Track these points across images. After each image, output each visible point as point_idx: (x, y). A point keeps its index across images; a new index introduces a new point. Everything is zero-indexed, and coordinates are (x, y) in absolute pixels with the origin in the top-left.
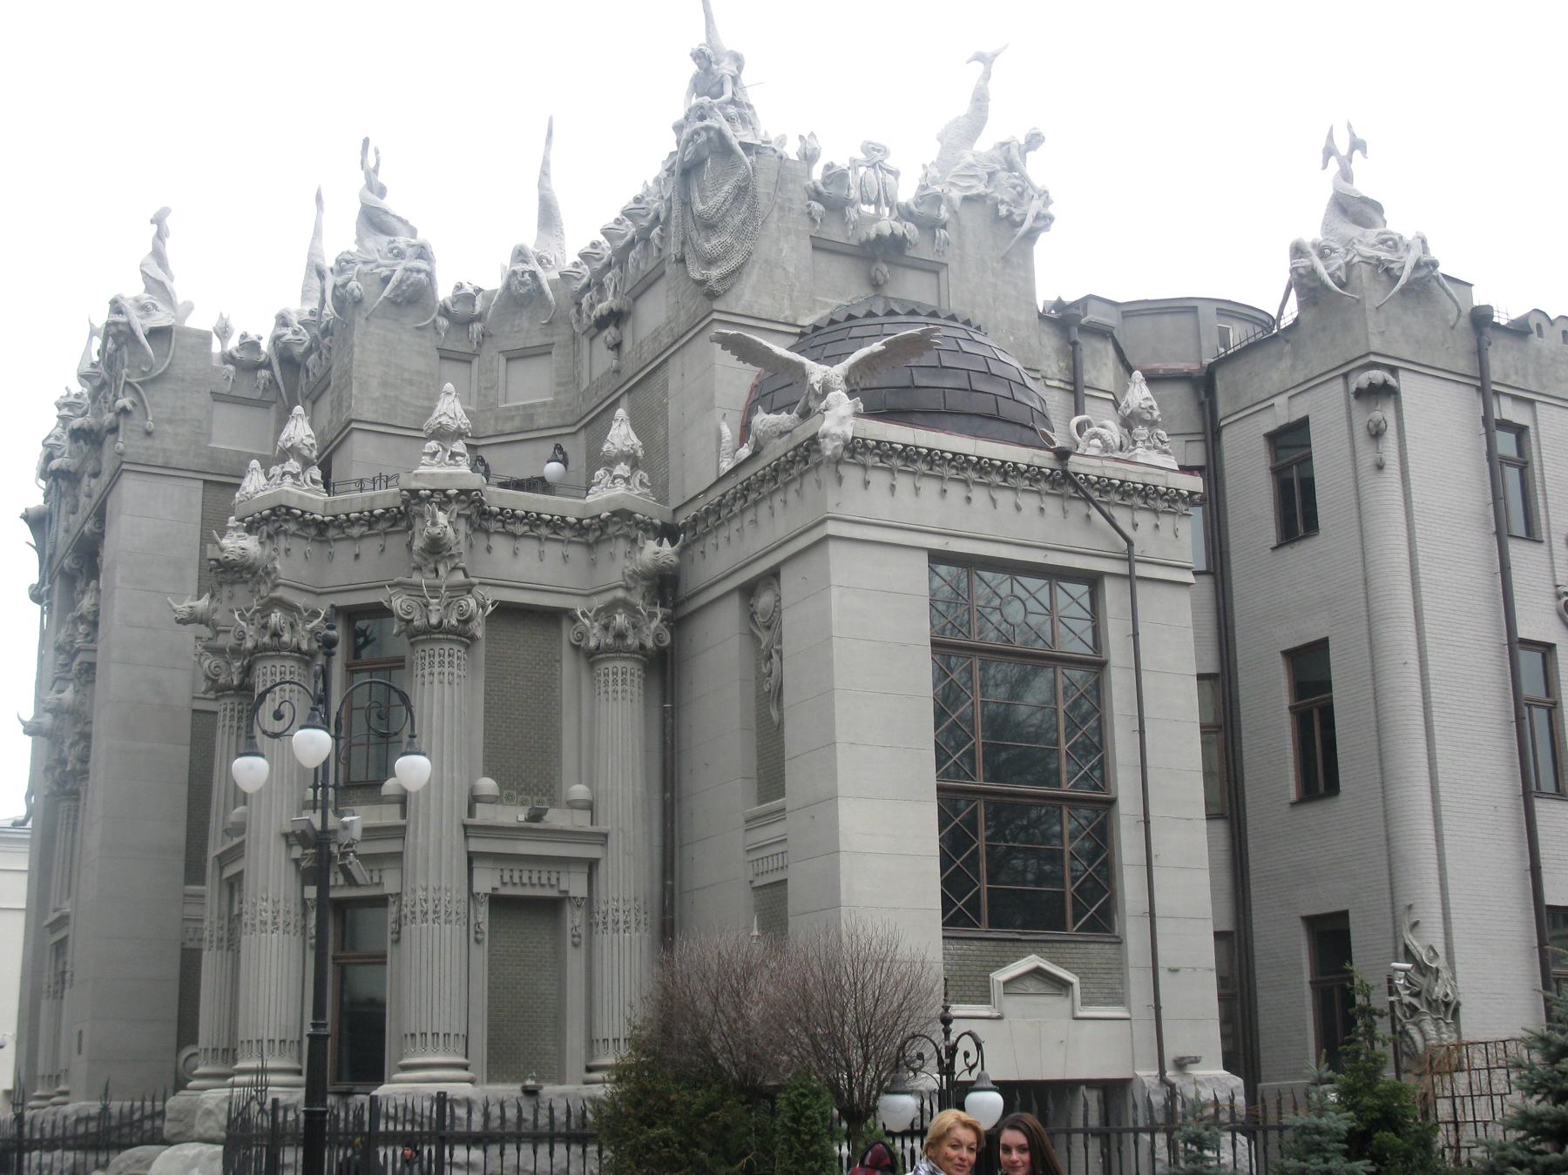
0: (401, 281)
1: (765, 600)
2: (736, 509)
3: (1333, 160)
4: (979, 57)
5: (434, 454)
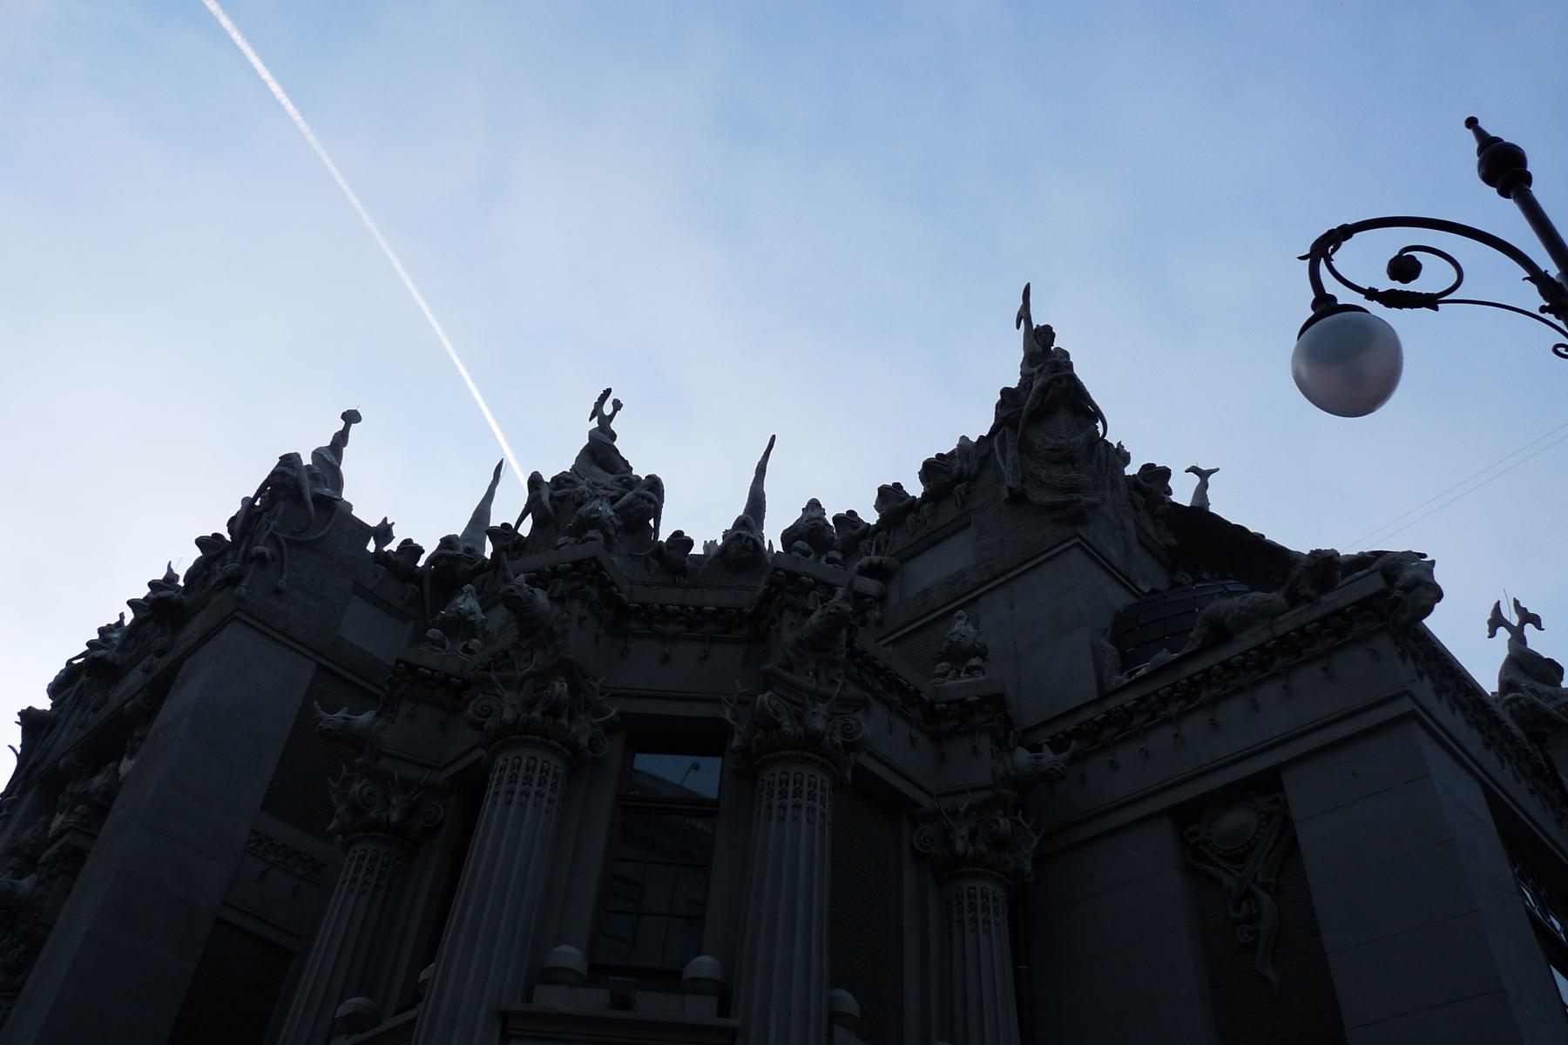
0: (630, 504)
1: (1238, 820)
2: (1173, 709)
3: (1502, 631)
4: (1194, 470)
5: (806, 554)
